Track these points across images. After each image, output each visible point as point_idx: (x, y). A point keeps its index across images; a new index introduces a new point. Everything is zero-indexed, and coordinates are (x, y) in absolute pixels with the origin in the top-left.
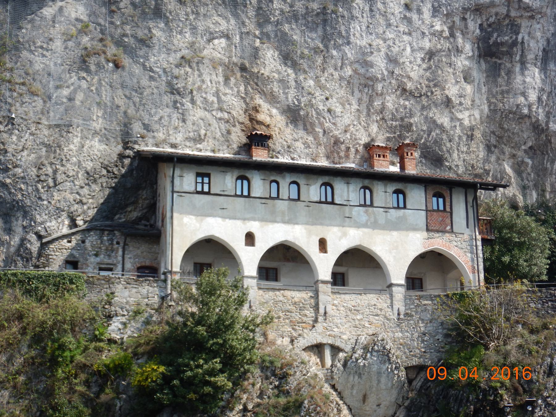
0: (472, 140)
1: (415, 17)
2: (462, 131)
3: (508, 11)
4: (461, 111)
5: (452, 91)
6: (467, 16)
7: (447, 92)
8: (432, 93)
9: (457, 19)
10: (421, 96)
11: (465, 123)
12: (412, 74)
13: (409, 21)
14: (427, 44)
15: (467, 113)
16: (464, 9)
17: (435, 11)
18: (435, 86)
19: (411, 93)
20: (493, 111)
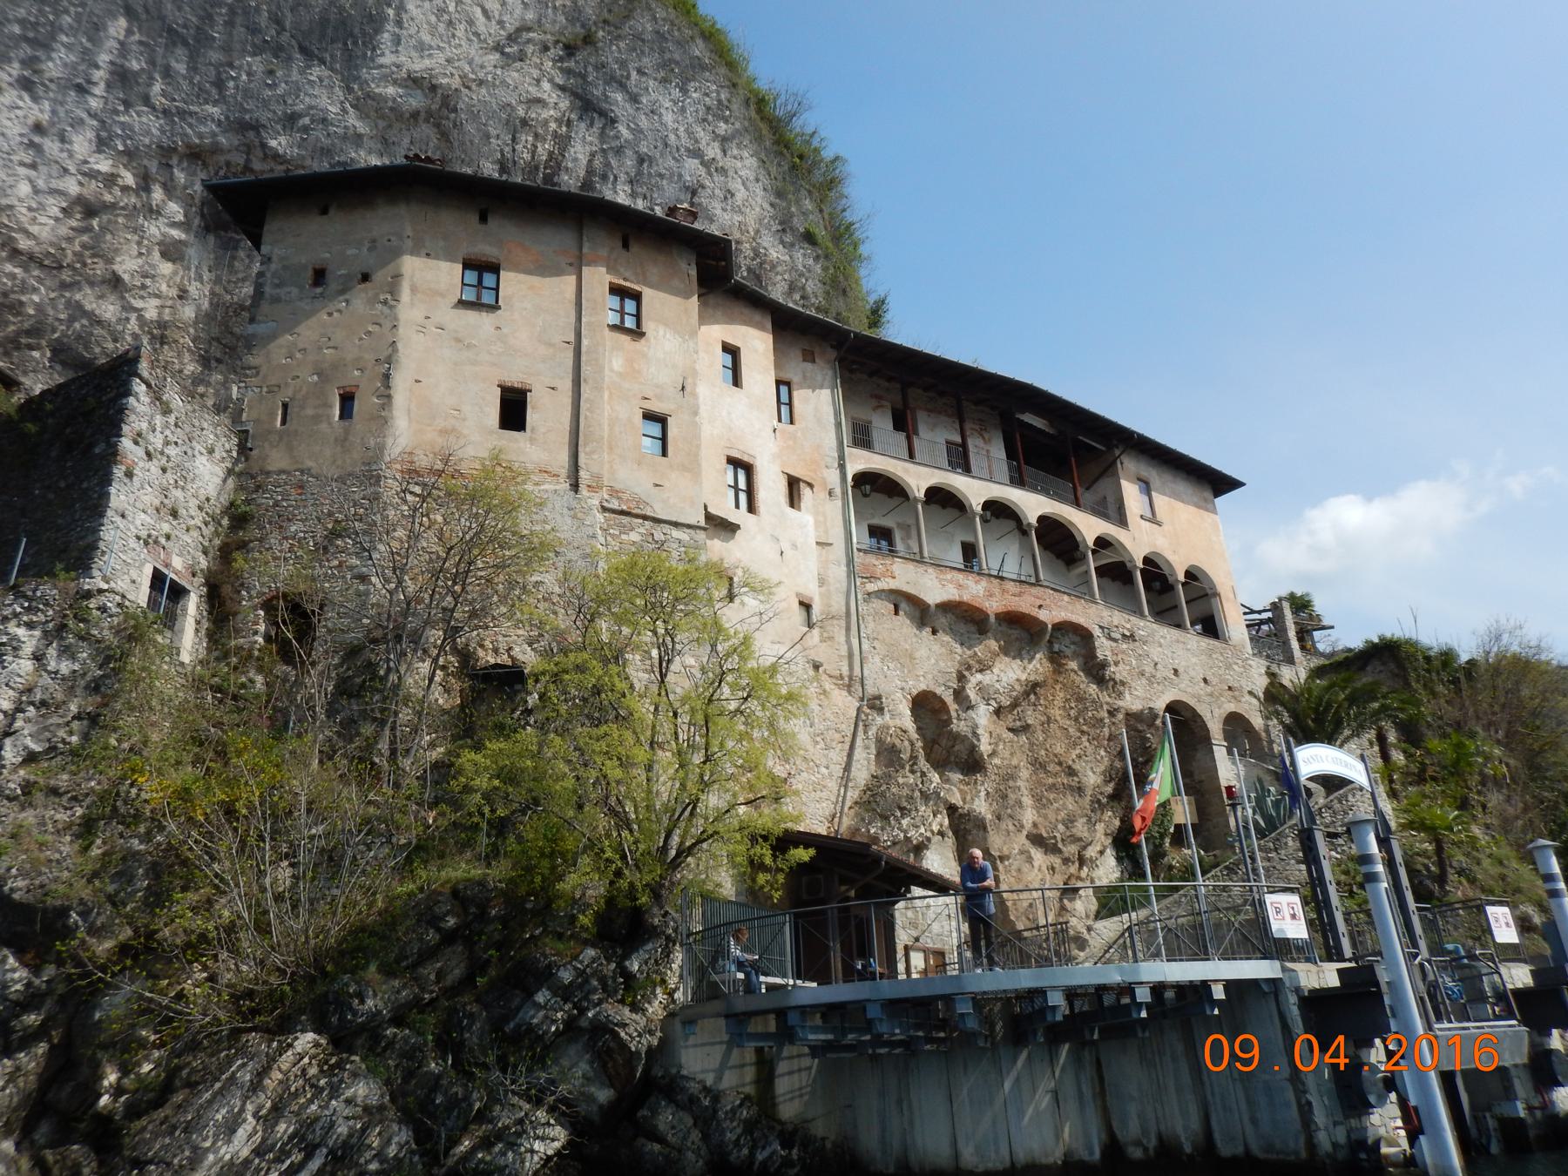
0: (162, 344)
1: (51, 146)
2: (141, 327)
3: (248, 161)
4: (142, 298)
5: (127, 266)
6: (174, 161)
7: (115, 267)
8: (85, 265)
9: (153, 166)
10: (61, 267)
11: (148, 316)
12: (34, 229)
13: (38, 148)
14: (72, 187)
15: (155, 302)
16: (160, 147)
17: (102, 144)
18: (94, 256)
19: (31, 257)
20: (215, 305)
